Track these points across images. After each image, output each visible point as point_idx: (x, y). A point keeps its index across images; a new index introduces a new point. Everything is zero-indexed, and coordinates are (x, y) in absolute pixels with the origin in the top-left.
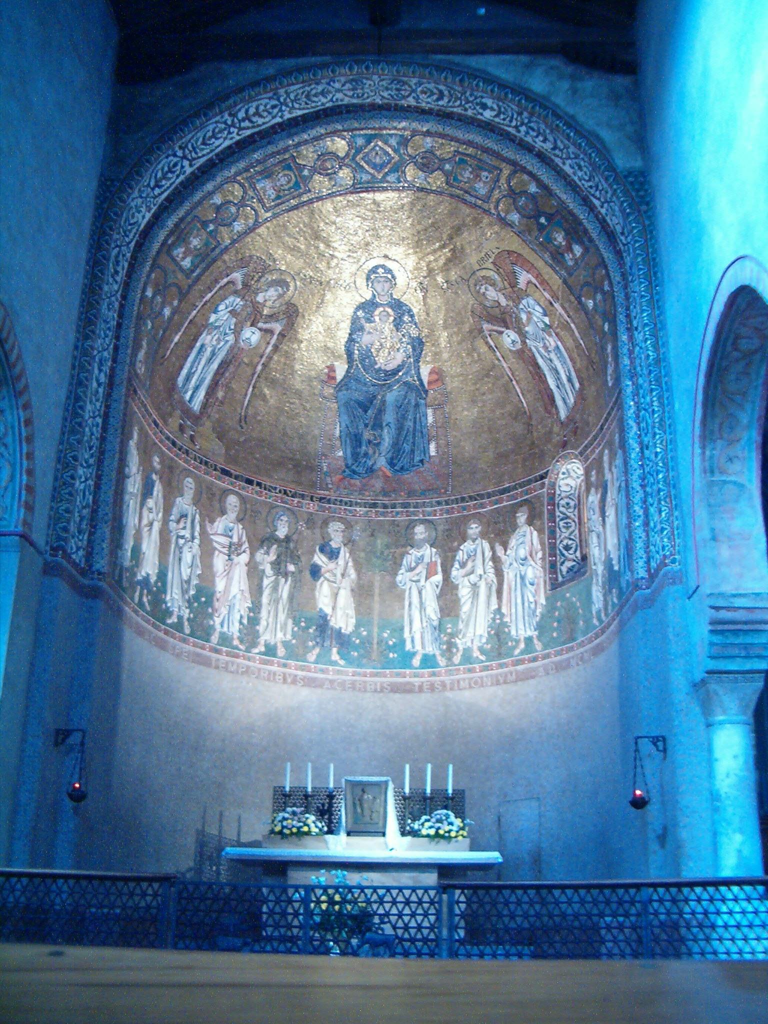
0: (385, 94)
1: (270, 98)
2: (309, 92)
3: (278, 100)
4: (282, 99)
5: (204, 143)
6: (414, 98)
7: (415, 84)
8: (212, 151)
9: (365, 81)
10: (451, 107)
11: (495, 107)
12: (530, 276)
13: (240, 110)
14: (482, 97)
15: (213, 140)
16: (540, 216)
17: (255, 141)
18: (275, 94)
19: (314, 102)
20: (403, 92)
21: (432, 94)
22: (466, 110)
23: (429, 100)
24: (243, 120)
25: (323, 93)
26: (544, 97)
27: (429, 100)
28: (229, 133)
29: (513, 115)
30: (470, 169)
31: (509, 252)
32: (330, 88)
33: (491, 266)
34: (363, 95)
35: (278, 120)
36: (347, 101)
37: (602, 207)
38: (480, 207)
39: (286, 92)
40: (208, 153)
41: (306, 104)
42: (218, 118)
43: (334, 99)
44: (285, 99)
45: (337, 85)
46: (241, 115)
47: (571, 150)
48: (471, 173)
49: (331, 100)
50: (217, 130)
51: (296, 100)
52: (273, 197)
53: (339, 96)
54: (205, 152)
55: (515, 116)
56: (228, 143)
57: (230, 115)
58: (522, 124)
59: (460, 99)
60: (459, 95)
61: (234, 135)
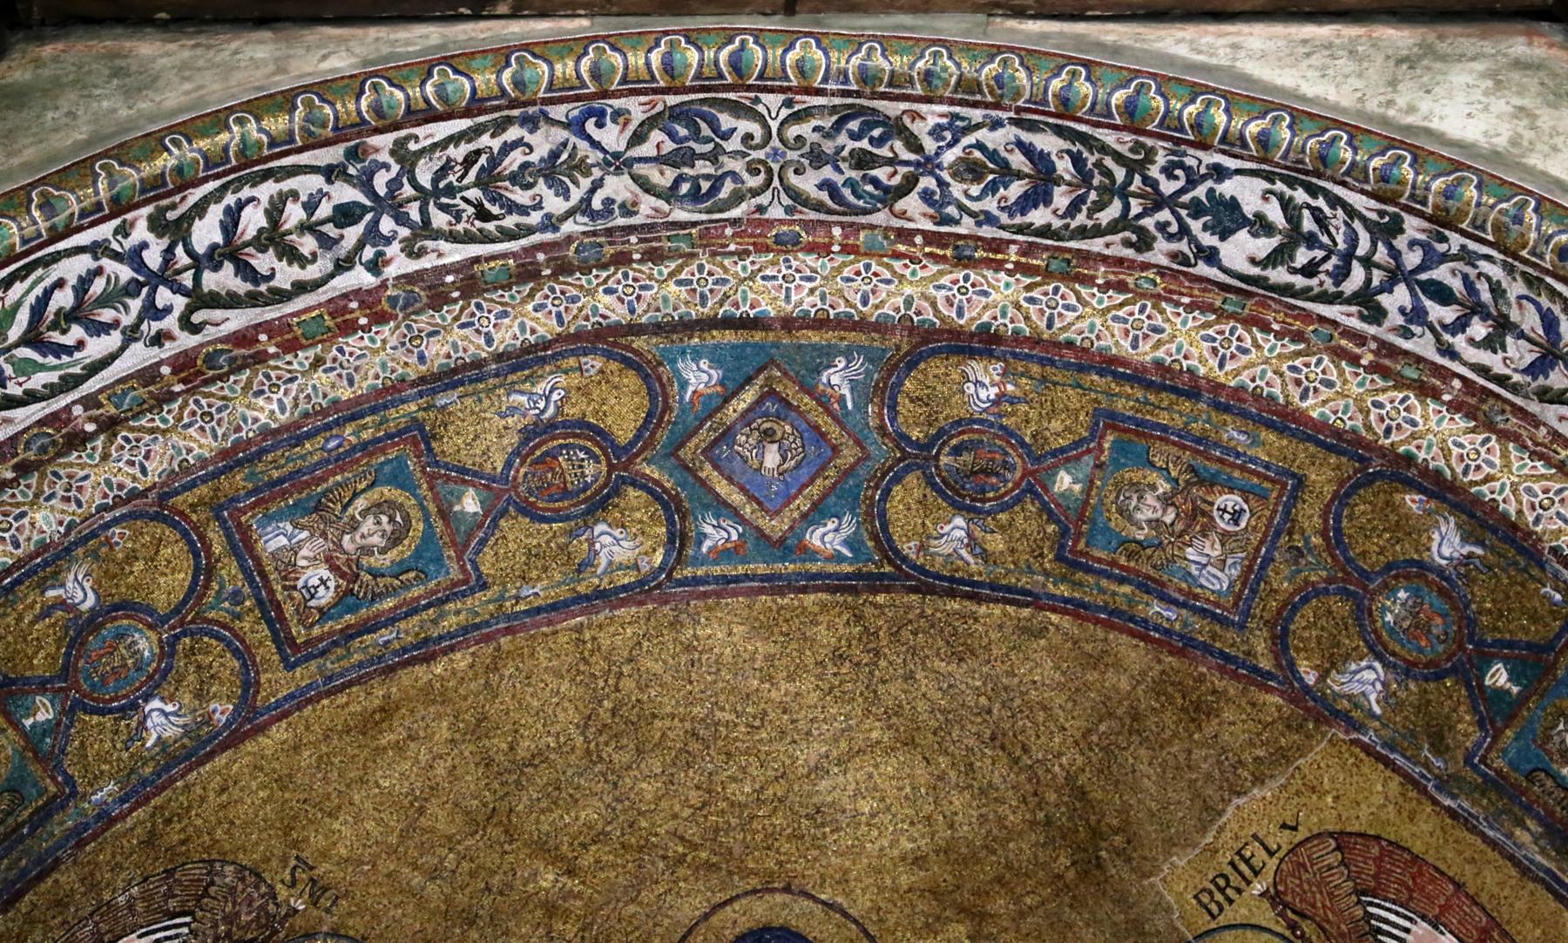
0: (807, 184)
1: (331, 173)
2: (494, 161)
3: (366, 185)
4: (380, 182)
5: (32, 338)
6: (926, 196)
8: (69, 383)
10: (1082, 233)
11: (1275, 213)
13: (200, 209)
15: (77, 332)
16: (1488, 660)
17: (261, 358)
18: (353, 155)
19: (513, 207)
21: (1007, 173)
22: (1144, 242)
23: (990, 204)
24: (213, 258)
25: (553, 170)
26: (1495, 156)
27: (990, 204)
28: (152, 311)
29: (1353, 241)
30: (1164, 487)
31: (1343, 840)
32: (583, 146)
33: (1266, 915)
35: (360, 278)
36: (648, 206)
38: (1207, 649)
39: (398, 150)
40: (53, 391)
41: (484, 215)
42: (105, 231)
43: (597, 204)
44: (394, 184)
45: (612, 137)
46: (206, 233)
48: (1167, 501)
49: (584, 207)
50: (98, 286)
51: (438, 192)
52: (325, 597)
53: (618, 187)
54: (38, 381)
55: (1363, 248)
56: (138, 356)
57: (158, 225)
58: (1396, 274)
59: (1124, 194)
61: (170, 322)
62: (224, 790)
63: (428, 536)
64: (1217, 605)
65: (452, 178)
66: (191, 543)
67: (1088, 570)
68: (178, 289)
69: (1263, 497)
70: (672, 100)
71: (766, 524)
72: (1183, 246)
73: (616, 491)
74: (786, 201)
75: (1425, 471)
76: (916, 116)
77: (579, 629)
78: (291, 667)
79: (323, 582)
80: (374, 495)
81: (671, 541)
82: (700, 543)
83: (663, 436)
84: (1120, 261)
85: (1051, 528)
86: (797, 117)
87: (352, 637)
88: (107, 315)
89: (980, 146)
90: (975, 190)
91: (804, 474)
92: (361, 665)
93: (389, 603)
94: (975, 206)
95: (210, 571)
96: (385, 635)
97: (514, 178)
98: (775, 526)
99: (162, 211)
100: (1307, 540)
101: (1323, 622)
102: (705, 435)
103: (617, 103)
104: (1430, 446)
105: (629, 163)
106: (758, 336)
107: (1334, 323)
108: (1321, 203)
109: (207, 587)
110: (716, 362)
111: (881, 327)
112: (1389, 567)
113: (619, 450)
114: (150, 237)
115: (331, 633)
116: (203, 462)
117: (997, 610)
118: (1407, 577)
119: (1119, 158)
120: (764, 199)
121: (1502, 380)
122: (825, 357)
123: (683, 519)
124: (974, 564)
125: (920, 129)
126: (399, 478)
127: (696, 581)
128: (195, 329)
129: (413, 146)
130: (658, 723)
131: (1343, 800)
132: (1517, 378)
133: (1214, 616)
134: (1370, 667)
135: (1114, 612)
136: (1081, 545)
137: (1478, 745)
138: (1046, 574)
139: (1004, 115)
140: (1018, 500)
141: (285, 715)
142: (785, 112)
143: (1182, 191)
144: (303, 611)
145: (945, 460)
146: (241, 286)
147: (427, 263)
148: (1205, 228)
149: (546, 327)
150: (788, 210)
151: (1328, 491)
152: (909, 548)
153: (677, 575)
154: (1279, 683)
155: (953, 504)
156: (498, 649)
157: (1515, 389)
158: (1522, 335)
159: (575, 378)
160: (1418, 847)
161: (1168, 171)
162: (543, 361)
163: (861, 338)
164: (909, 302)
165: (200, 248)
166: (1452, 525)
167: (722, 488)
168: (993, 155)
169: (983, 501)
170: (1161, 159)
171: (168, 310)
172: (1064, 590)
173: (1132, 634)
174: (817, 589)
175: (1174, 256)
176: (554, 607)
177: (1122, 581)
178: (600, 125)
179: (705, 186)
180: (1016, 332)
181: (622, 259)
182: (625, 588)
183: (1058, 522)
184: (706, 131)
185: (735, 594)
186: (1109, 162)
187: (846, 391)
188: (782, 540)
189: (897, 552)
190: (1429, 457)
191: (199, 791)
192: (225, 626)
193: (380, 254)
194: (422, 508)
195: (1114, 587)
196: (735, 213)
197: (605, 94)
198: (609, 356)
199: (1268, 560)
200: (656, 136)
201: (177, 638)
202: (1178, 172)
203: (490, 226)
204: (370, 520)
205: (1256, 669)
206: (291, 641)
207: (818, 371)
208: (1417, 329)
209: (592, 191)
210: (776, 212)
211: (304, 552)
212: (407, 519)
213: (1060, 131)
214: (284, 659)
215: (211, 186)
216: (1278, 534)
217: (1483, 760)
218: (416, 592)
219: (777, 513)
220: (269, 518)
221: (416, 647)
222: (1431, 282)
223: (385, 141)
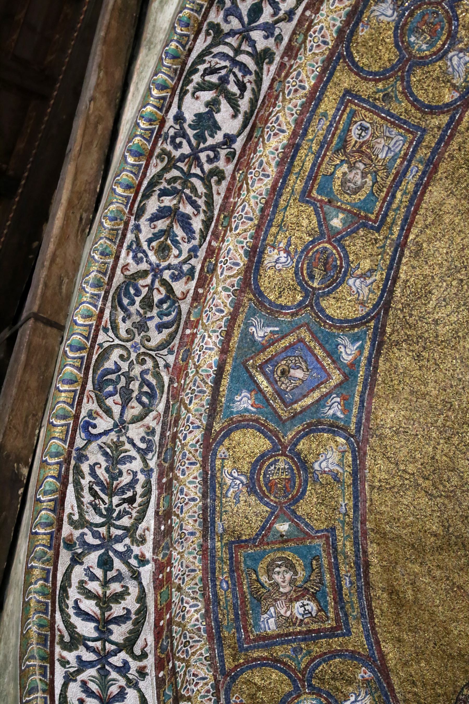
4: (90, 539)
6: (175, 278)
7: (138, 261)
9: (109, 365)
10: (210, 204)
11: (207, 96)
13: (70, 627)
14: (179, 118)
18: (69, 545)
20: (157, 297)
23: (185, 247)
29: (224, 56)
30: (345, 168)
34: (144, 382)
39: (75, 525)
41: (131, 500)
42: (59, 672)
43: (143, 446)
44: (96, 535)
48: (352, 167)
49: (143, 453)
52: (312, 607)
59: (189, 175)
60: (175, 173)
61: (134, 665)
62: (414, 683)
63: (296, 551)
64: (411, 143)
65: (102, 507)
66: (255, 666)
67: (386, 215)
68: (115, 653)
69: (353, 113)
70: (90, 386)
71: (333, 383)
72: (223, 153)
73: (298, 454)
74: (165, 352)
75: (347, 23)
76: (125, 267)
77: (372, 488)
78: (349, 633)
79: (303, 606)
80: (261, 571)
81: (334, 432)
82: (338, 418)
83: (272, 425)
84: (229, 190)
85: (361, 233)
86: (115, 328)
87: (341, 599)
88: (114, 690)
89: (150, 241)
90: (175, 252)
91: (310, 358)
92: (360, 598)
93: (327, 577)
94: (185, 255)
95: (277, 660)
96: (346, 583)
97: (113, 478)
98: (336, 377)
99: (62, 641)
100: (379, 91)
101: (425, 86)
102: (277, 405)
103: (83, 413)
104: (334, 19)
105: (122, 421)
106: (228, 368)
107: (273, 80)
108: (201, 68)
109: (285, 664)
110: (239, 391)
111: (237, 306)
112: (397, 46)
113: (274, 449)
114: (75, 653)
115: (335, 608)
116: (211, 649)
117: (404, 268)
118: (403, 35)
119: (165, 170)
120: (161, 363)
122: (246, 334)
123: (321, 424)
124: (377, 276)
125: (133, 268)
126: (256, 559)
127: (359, 423)
128: (144, 655)
129: (76, 517)
130: (438, 457)
133: (417, 146)
134: (451, 60)
135: (411, 201)
136: (373, 217)
138: (386, 238)
139: (132, 222)
140: (343, 248)
141: (378, 643)
142: (110, 333)
143: (189, 142)
144: (315, 619)
145: (315, 285)
146: (128, 626)
147: (150, 537)
148: (212, 136)
149: (196, 471)
150: (171, 352)
151: (354, 77)
152: (361, 312)
153: (353, 433)
154: (457, 113)
155: (340, 284)
156: (373, 530)
159: (229, 464)
161: (178, 146)
162: (214, 476)
163: (241, 317)
164: (226, 289)
165: (95, 635)
166: (375, 8)
167: (308, 401)
168: (156, 236)
169: (341, 267)
170: (169, 148)
171: (125, 663)
172: (396, 229)
173: (423, 193)
174: (377, 362)
175: (229, 159)
176: (356, 498)
177: (394, 196)
178: (95, 426)
179: (146, 389)
180: (252, 237)
181: (175, 436)
182: (354, 460)
183: (358, 228)
184: (113, 377)
185: (370, 403)
186: (168, 176)
187: (269, 329)
188: (345, 375)
189: (363, 317)
190: (340, 20)
191: (410, 695)
192: (313, 660)
193: (136, 557)
194: (278, 549)
195: (397, 201)
196: (166, 379)
197: (76, 417)
198: (220, 443)
199: (388, 113)
200: (109, 402)
201: (310, 685)
202: (178, 140)
203: (139, 500)
204: (276, 576)
205: (448, 125)
206: (332, 629)
207: (254, 342)
208: (277, 32)
209: (134, 445)
210: (171, 359)
211: (282, 612)
212: (281, 559)
213: (146, 196)
214: (343, 635)
215: (58, 615)
216: (375, 106)
218: (325, 562)
219: (329, 375)
220: (256, 625)
221: (358, 569)
222: (249, 15)
223: (66, 530)
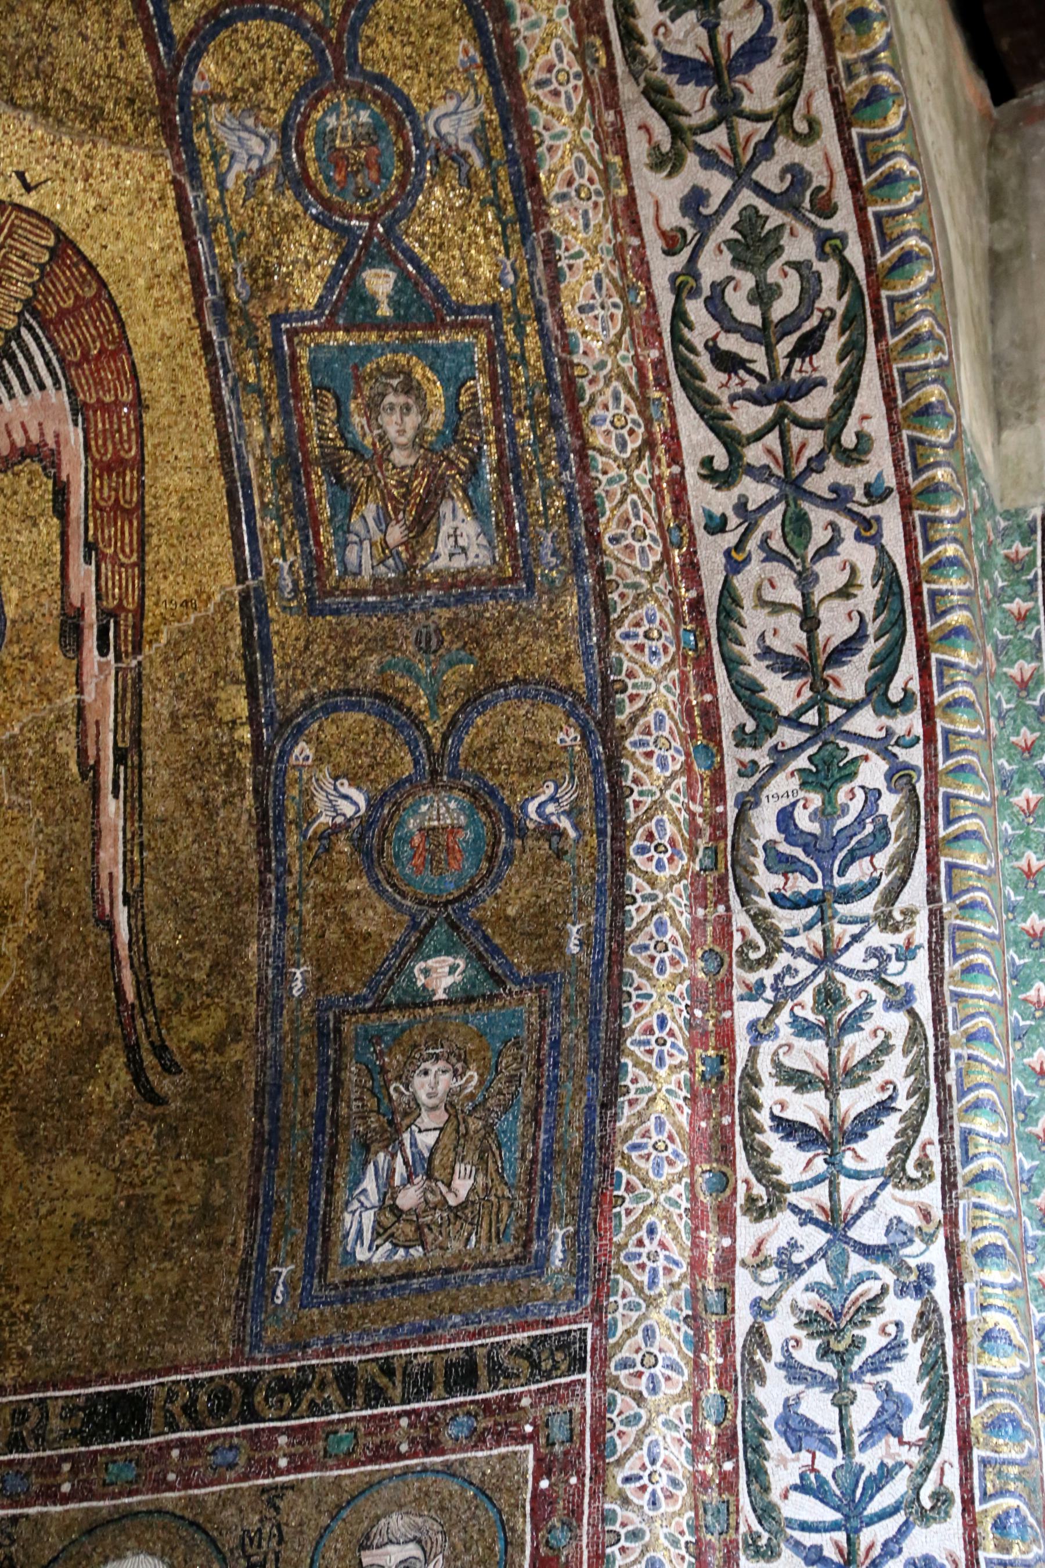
12: (75, 436)
37: (723, 479)
47: (786, 152)
75: (505, 40)
101: (270, 53)
104: (535, 25)
112: (380, 79)
118: (387, 108)
121: (630, 36)
131: (107, 218)
132: (650, 50)
134: (265, 141)
137: (302, 316)
154: (167, 54)
157: (633, 57)
158: (712, 29)
160: (135, 332)
166: (477, 112)
190: (524, 33)
205: (164, 19)
217: (293, 333)
